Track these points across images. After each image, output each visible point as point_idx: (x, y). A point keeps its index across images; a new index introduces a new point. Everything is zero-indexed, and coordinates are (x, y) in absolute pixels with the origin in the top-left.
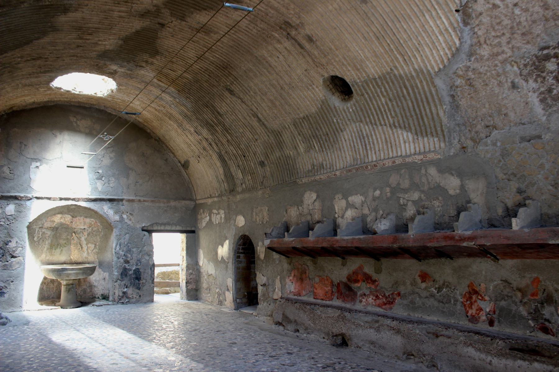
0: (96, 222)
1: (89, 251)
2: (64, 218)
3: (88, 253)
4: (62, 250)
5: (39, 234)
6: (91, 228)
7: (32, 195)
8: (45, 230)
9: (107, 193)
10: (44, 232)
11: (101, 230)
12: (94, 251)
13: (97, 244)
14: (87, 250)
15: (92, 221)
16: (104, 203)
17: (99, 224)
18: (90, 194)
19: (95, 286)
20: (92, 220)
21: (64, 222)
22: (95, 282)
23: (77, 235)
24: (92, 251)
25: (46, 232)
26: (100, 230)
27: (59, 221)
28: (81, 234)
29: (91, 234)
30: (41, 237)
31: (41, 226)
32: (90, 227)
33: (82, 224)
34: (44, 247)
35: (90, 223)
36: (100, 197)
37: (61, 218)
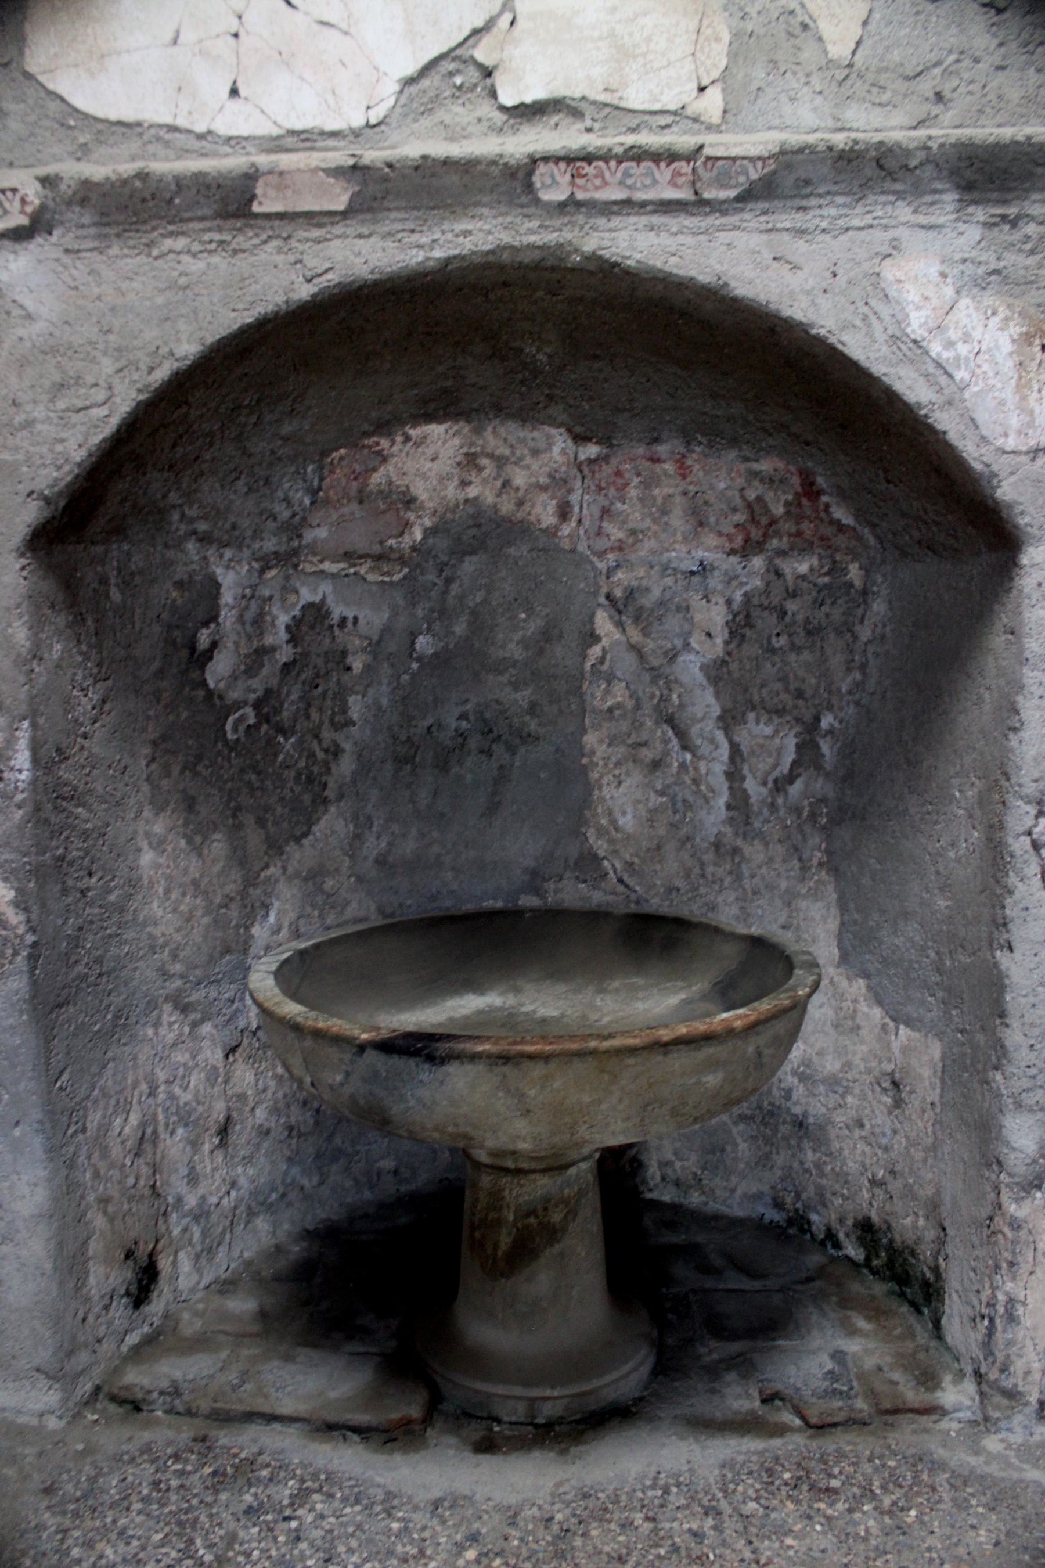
0: (810, 491)
1: (751, 785)
2: (501, 462)
3: (739, 803)
4: (502, 776)
5: (259, 623)
6: (758, 562)
7: (42, 171)
8: (326, 588)
9: (926, 86)
10: (316, 612)
11: (866, 570)
12: (796, 788)
13: (827, 721)
14: (734, 776)
15: (770, 481)
16: (903, 212)
17: (841, 514)
18: (712, 104)
19: (800, 1124)
20: (765, 466)
21: (506, 507)
22: (800, 1091)
23: (635, 635)
24: (780, 785)
25: (337, 611)
26: (854, 573)
27: (451, 491)
28: (673, 623)
29: (768, 622)
30: (285, 654)
31: (270, 544)
32: (747, 549)
33: (677, 520)
34: (336, 752)
35: (755, 509)
36: (839, 140)
37: (471, 461)
